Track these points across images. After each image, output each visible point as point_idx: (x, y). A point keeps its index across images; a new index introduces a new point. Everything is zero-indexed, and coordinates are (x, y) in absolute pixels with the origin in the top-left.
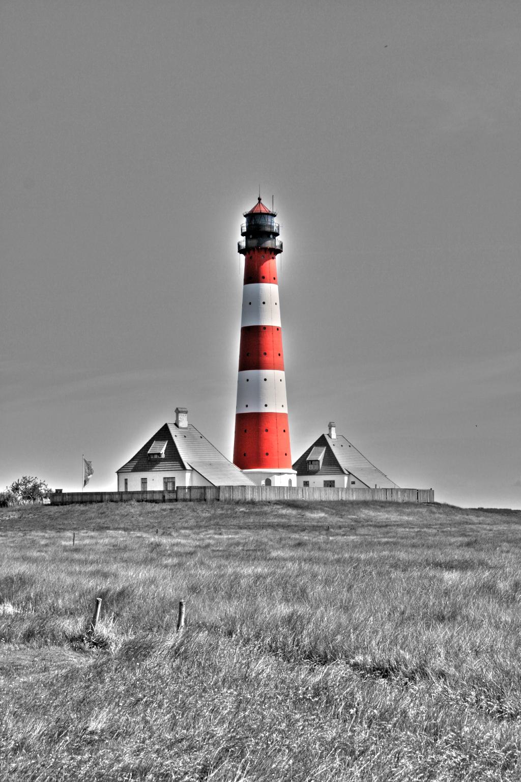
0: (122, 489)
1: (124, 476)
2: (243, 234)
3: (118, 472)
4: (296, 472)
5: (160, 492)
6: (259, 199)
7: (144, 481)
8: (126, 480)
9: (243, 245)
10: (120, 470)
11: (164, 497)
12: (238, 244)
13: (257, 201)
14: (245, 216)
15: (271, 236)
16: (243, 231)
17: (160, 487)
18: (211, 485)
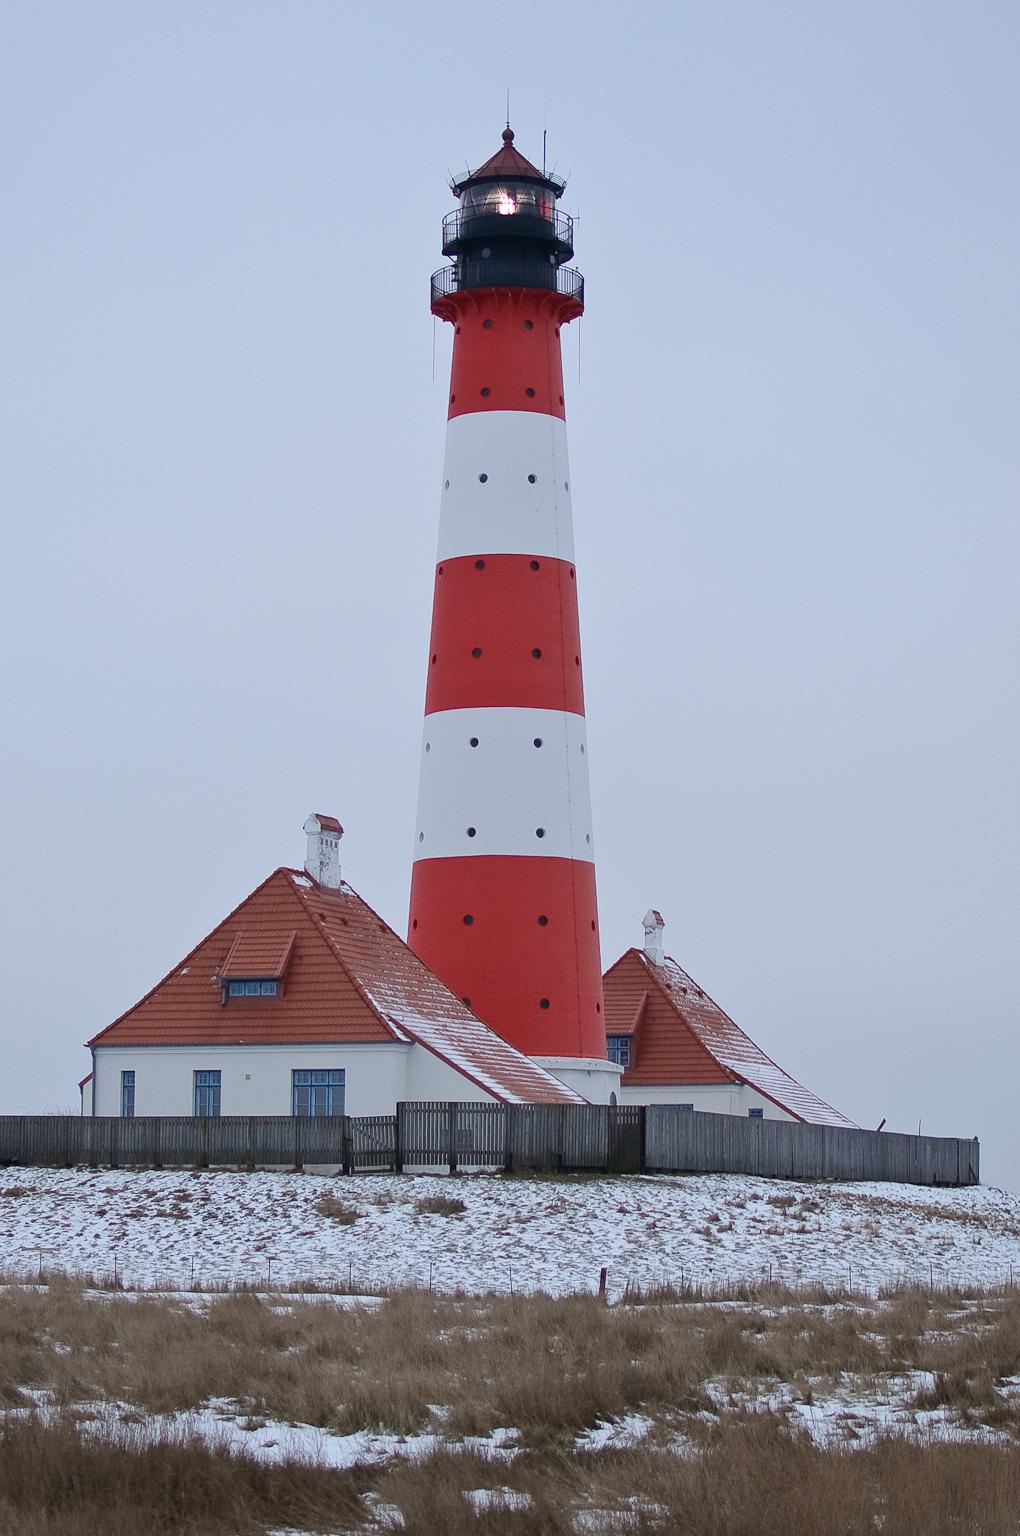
0: (111, 1108)
1: (116, 1061)
2: (446, 252)
3: (94, 1044)
4: (621, 1069)
5: (280, 1120)
6: (508, 136)
7: (207, 1083)
8: (128, 1076)
9: (450, 287)
10: (99, 1037)
11: (346, 1141)
12: (432, 279)
13: (501, 144)
14: (459, 189)
15: (552, 260)
16: (451, 237)
17: (279, 1103)
18: (496, 1101)
